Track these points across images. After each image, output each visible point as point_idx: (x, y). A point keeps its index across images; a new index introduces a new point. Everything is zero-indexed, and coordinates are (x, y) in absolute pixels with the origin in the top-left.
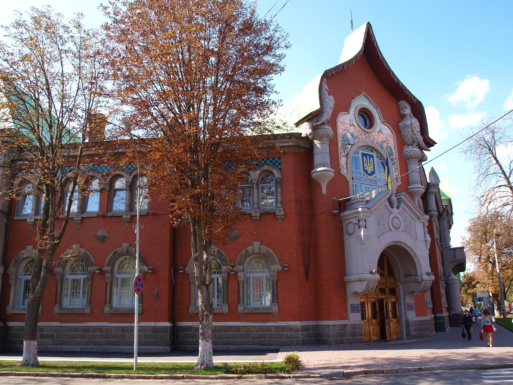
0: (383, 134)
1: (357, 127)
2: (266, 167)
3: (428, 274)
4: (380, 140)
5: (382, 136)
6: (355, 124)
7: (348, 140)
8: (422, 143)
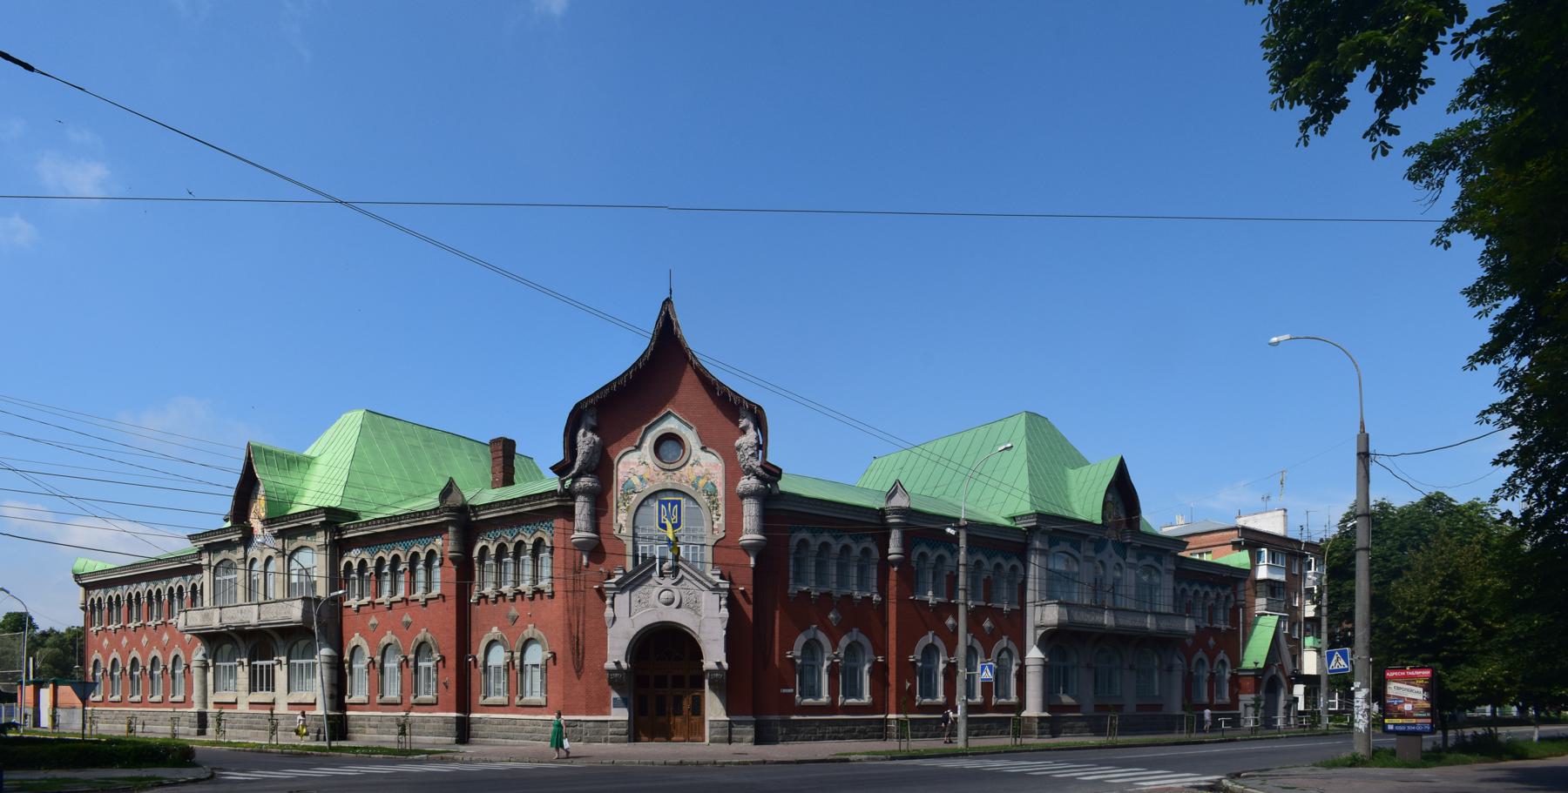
0: (704, 467)
1: (652, 465)
2: (539, 534)
3: (719, 664)
4: (693, 477)
5: (697, 469)
6: (649, 461)
7: (633, 487)
8: (760, 471)
